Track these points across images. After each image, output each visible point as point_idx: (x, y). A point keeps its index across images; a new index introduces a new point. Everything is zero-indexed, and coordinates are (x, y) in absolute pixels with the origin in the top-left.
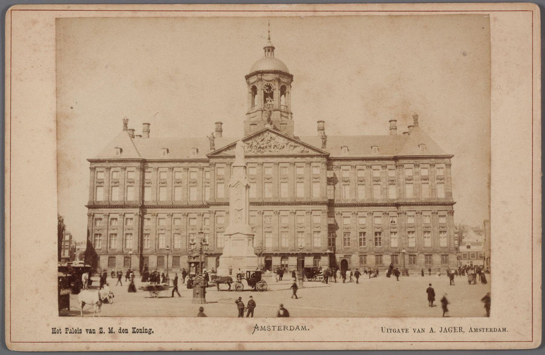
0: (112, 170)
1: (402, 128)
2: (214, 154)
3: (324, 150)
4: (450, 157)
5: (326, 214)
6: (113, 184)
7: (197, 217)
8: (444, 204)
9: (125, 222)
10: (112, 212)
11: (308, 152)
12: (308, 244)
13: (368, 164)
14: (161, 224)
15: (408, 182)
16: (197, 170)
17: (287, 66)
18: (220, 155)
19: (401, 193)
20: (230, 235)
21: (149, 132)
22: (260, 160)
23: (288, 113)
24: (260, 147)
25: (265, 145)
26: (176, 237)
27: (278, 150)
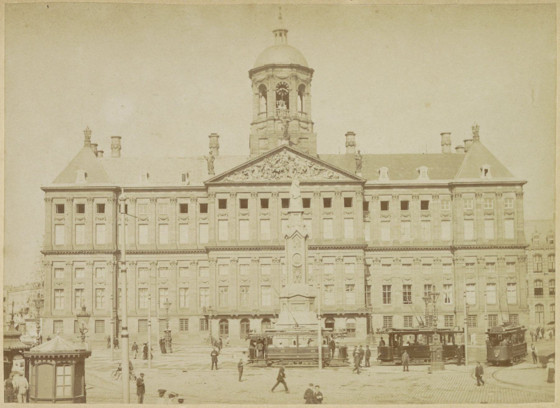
2: (214, 181)
3: (359, 175)
11: (338, 178)
13: (414, 193)
15: (467, 217)
18: (221, 181)
21: (120, 149)
23: (308, 123)
24: (275, 171)
25: (281, 168)
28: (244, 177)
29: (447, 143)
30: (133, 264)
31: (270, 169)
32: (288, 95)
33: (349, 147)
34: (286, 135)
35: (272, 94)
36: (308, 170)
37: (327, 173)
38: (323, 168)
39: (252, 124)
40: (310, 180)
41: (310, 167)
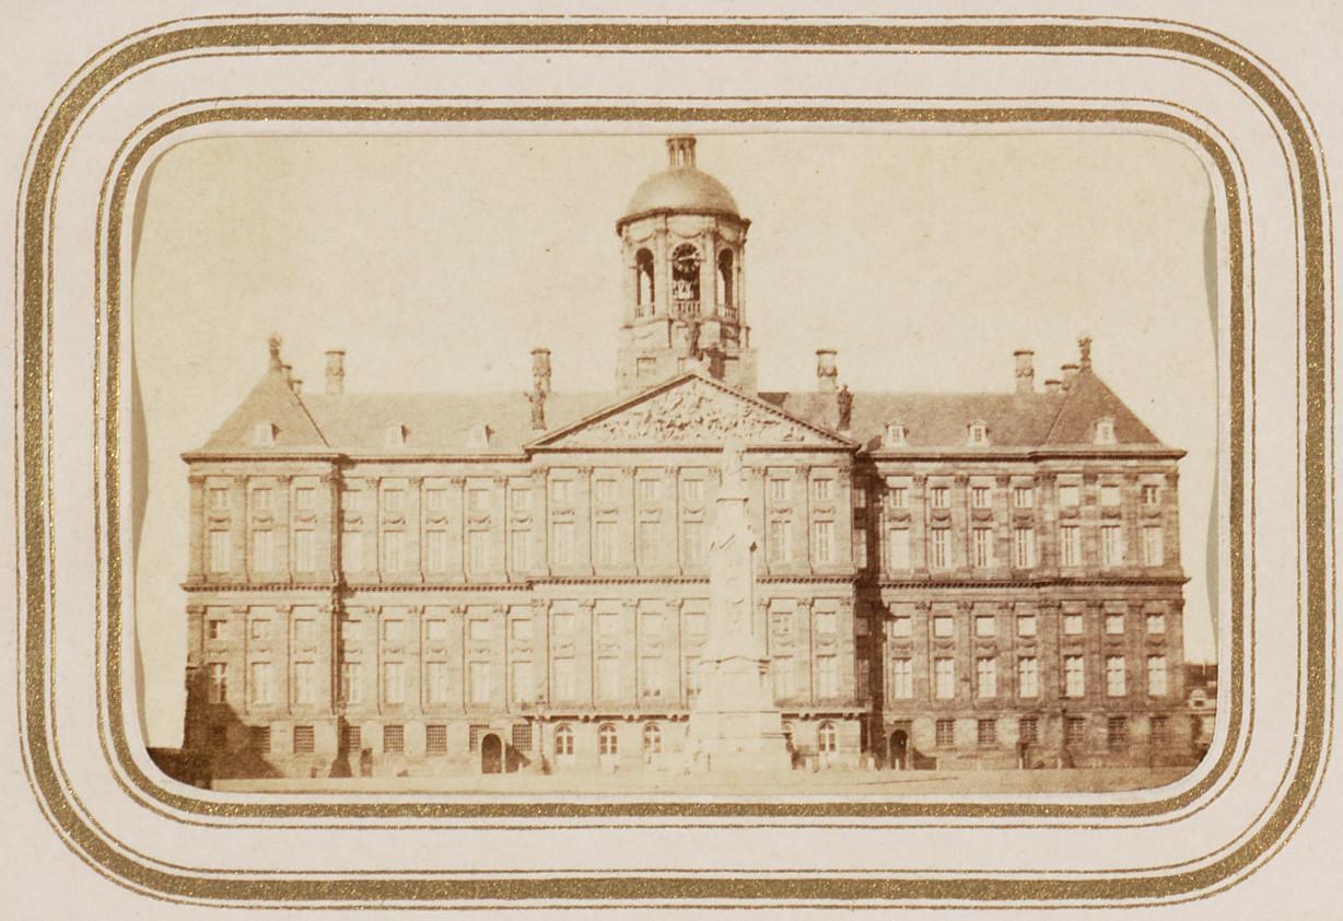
0: (251, 485)
2: (544, 443)
3: (846, 435)
4: (1177, 456)
5: (850, 609)
6: (257, 525)
8: (1159, 582)
10: (257, 602)
11: (803, 439)
12: (802, 690)
14: (390, 636)
15: (1066, 522)
16: (489, 484)
17: (735, 194)
19: (1048, 554)
20: (719, 662)
27: (719, 433)
30: (373, 611)
32: (698, 268)
34: (696, 351)
35: (663, 267)
38: (772, 417)
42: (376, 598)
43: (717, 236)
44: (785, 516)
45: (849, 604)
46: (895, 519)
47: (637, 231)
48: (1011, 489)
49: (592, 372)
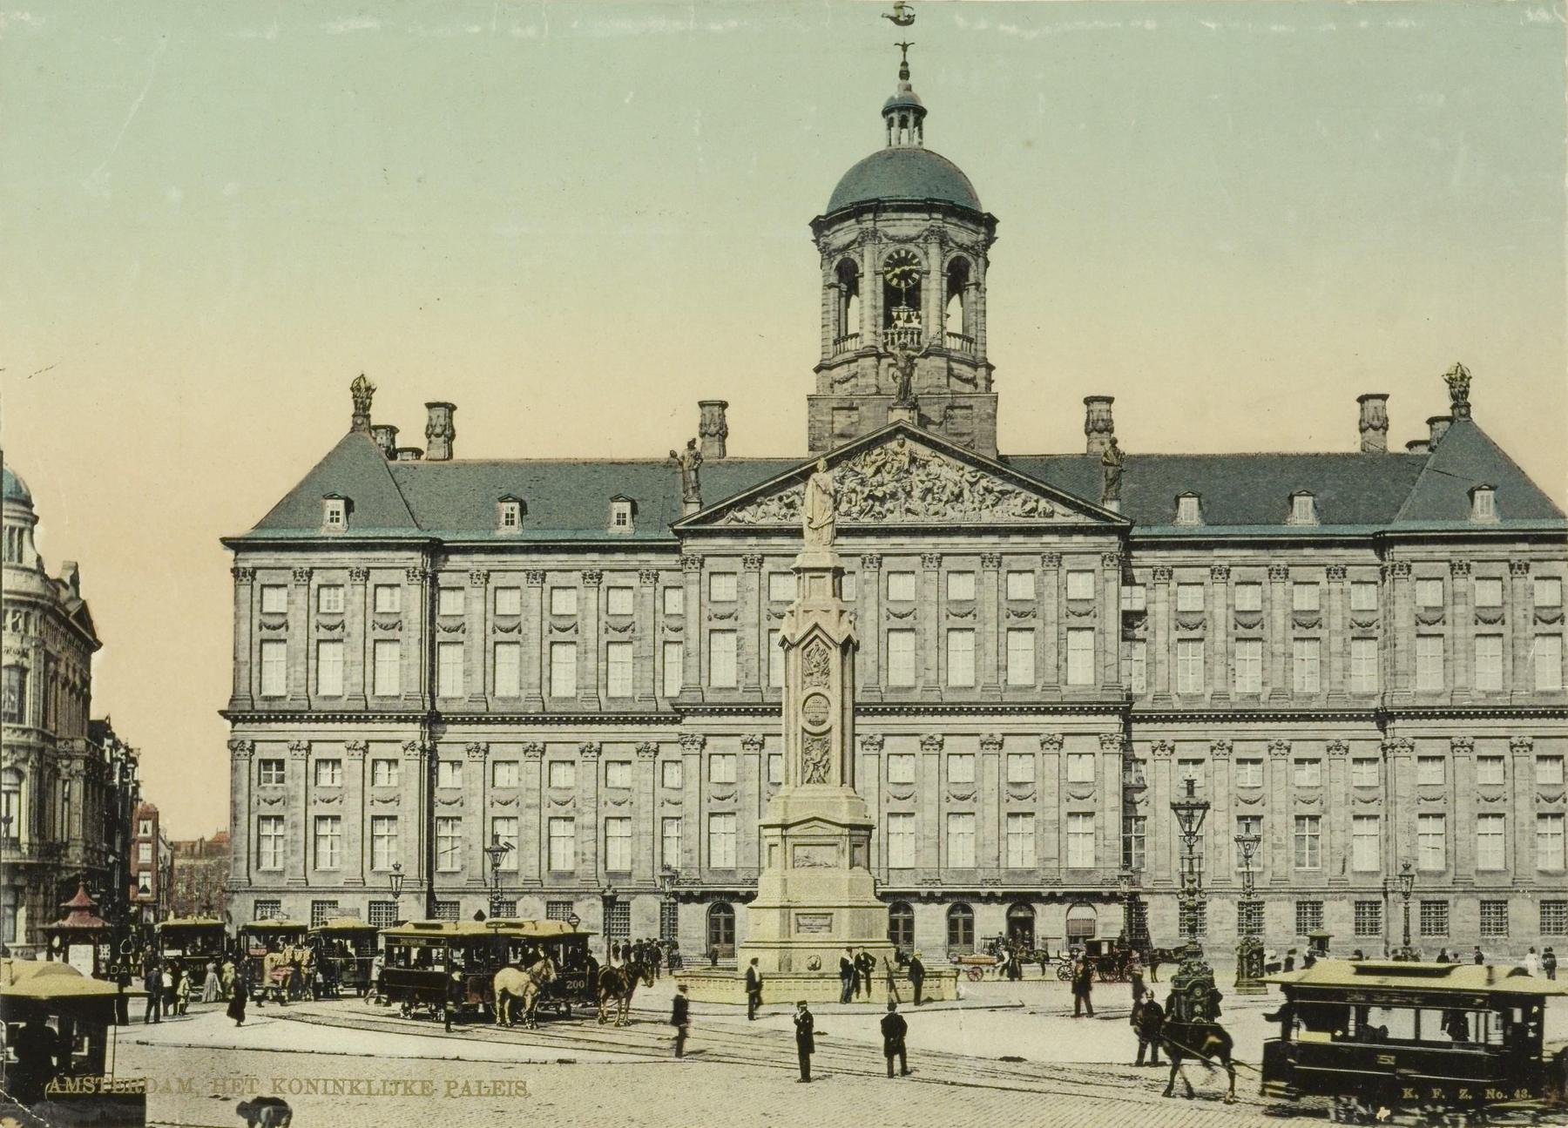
0: (317, 579)
1: (1406, 427)
2: (696, 522)
3: (1113, 506)
7: (632, 756)
9: (368, 775)
11: (1052, 514)
16: (633, 580)
18: (720, 524)
22: (871, 544)
23: (975, 366)
25: (889, 488)
26: (559, 828)
28: (784, 510)
29: (1376, 423)
30: (478, 749)
31: (859, 488)
32: (918, 286)
33: (1095, 434)
34: (906, 397)
36: (966, 494)
37: (1019, 501)
38: (1009, 487)
39: (818, 370)
40: (972, 520)
41: (972, 484)
42: (480, 734)
43: (943, 241)
44: (1033, 623)
45: (1111, 742)
46: (1186, 626)
47: (844, 235)
48: (1348, 584)
49: (771, 429)
